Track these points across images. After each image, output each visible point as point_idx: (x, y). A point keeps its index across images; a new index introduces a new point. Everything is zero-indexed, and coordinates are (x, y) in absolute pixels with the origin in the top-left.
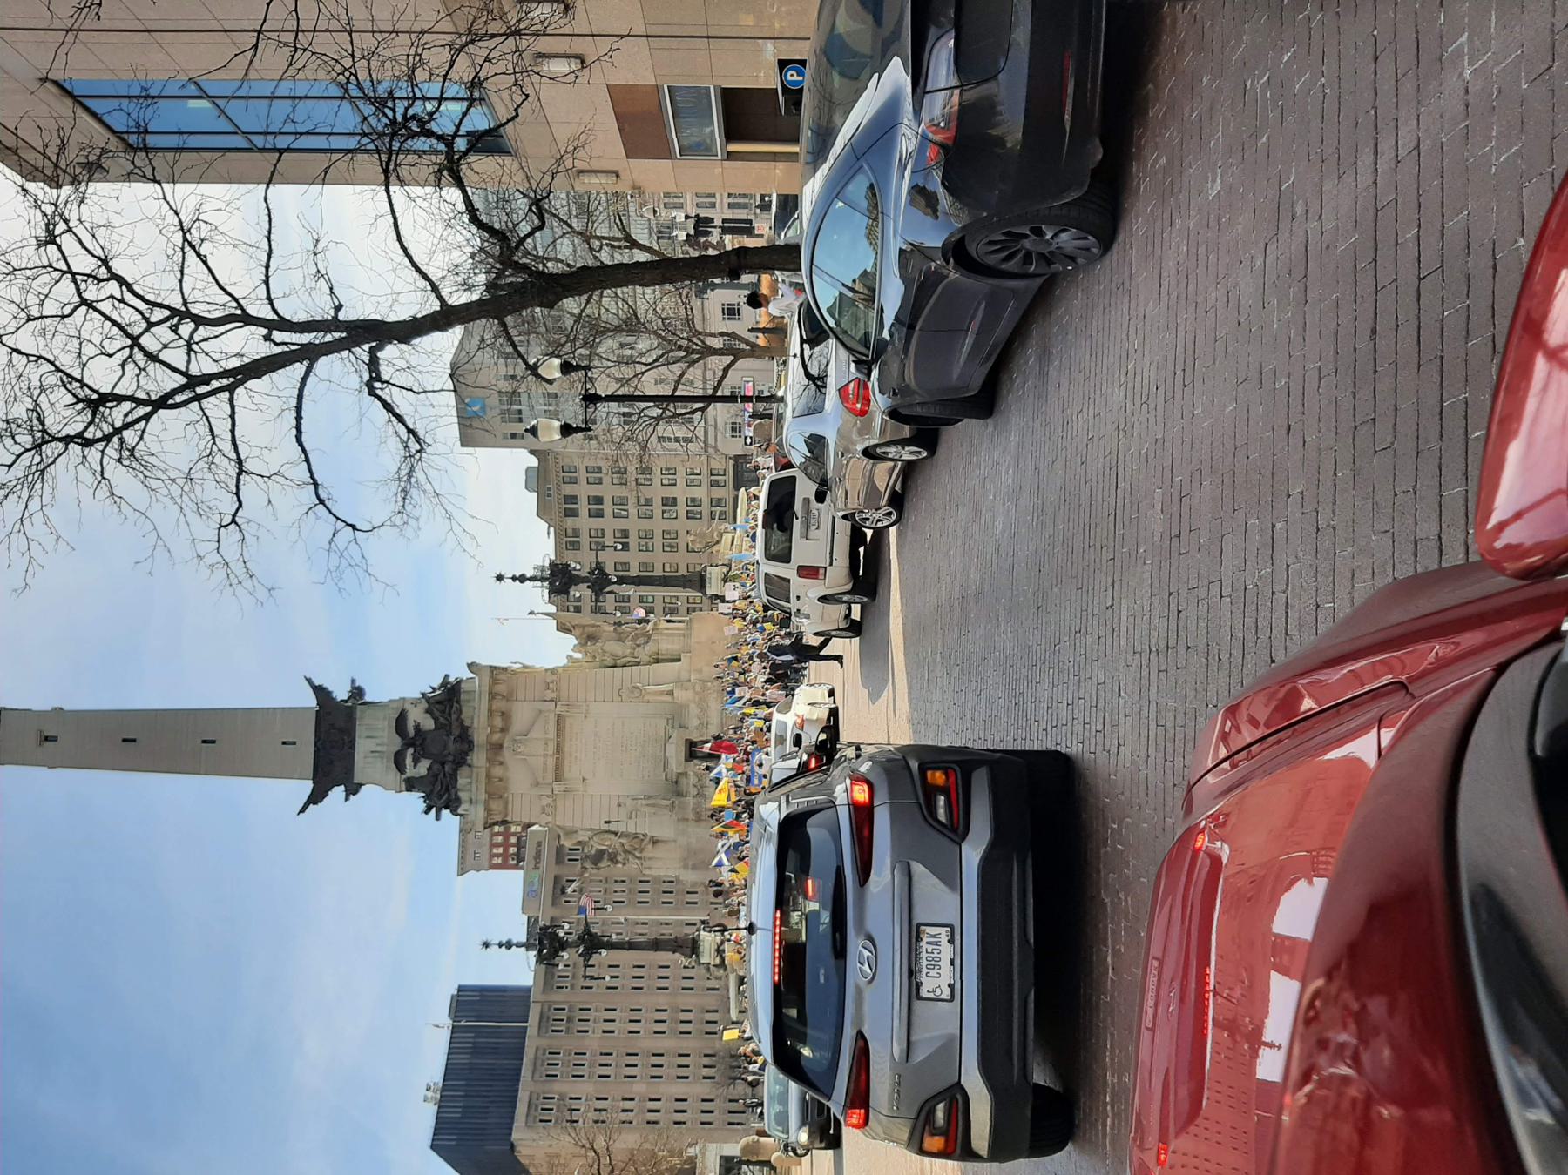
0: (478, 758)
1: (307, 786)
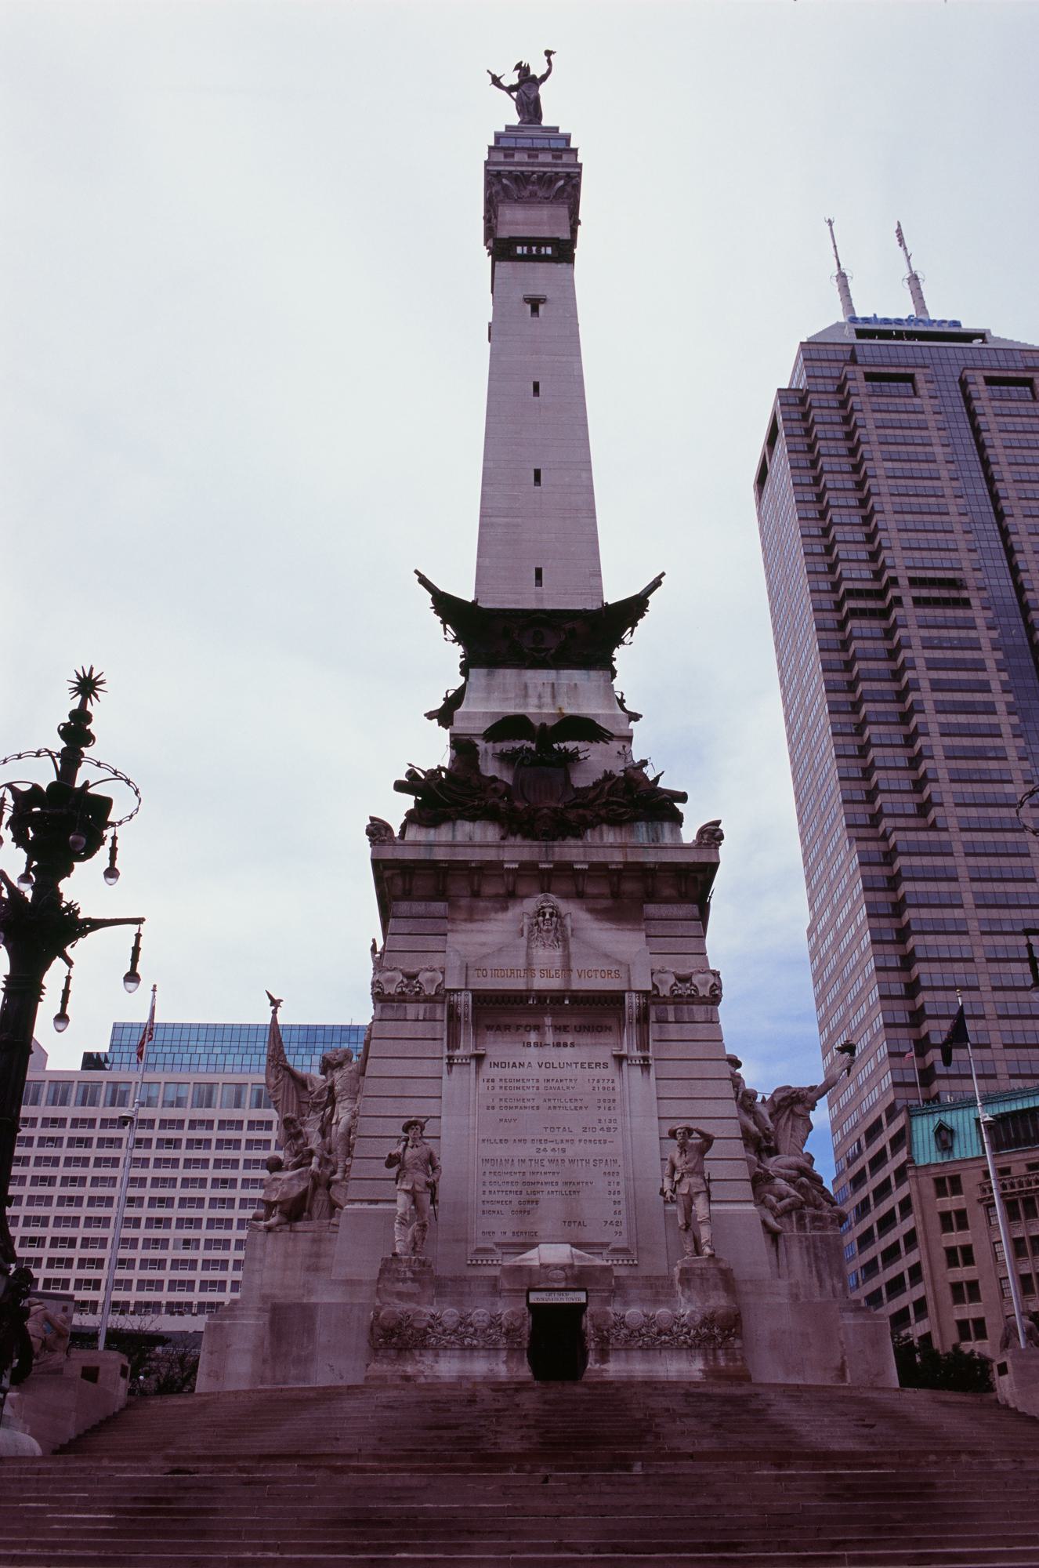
0: (517, 852)
1: (466, 592)
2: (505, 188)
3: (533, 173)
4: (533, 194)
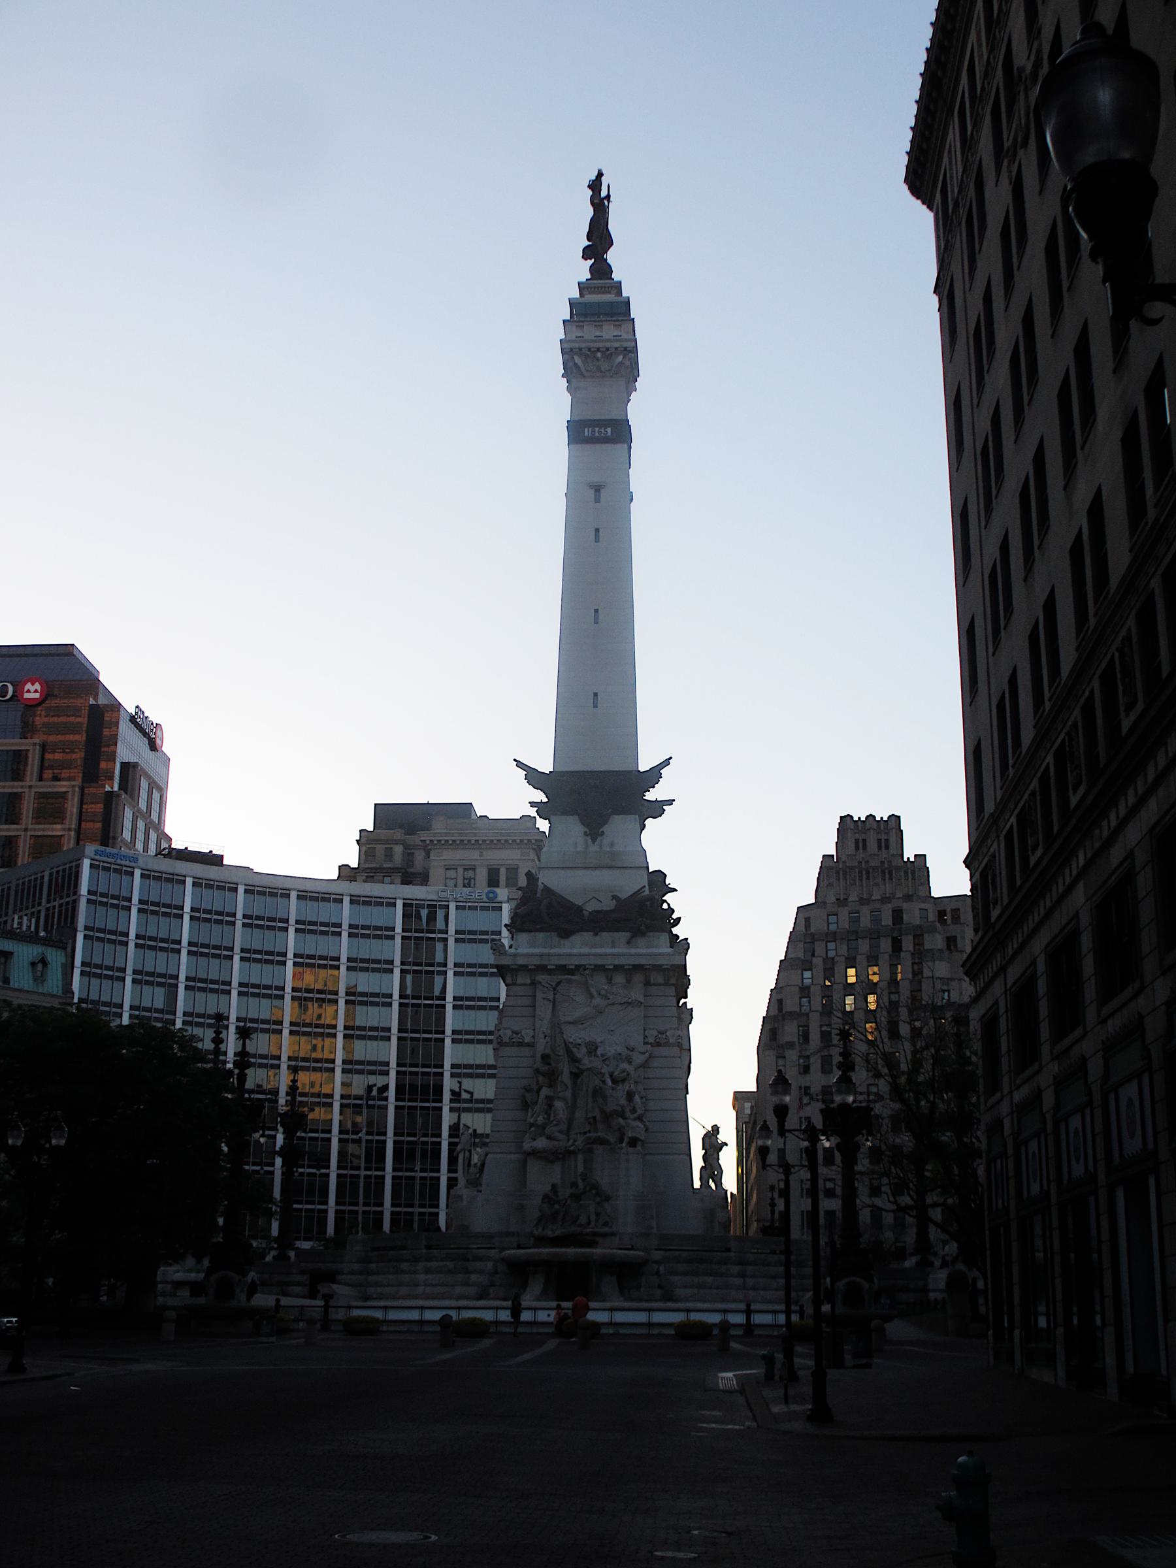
1: (546, 765)
2: (576, 364)
3: (598, 350)
4: (599, 369)
